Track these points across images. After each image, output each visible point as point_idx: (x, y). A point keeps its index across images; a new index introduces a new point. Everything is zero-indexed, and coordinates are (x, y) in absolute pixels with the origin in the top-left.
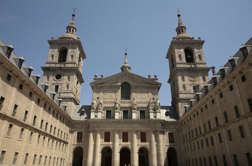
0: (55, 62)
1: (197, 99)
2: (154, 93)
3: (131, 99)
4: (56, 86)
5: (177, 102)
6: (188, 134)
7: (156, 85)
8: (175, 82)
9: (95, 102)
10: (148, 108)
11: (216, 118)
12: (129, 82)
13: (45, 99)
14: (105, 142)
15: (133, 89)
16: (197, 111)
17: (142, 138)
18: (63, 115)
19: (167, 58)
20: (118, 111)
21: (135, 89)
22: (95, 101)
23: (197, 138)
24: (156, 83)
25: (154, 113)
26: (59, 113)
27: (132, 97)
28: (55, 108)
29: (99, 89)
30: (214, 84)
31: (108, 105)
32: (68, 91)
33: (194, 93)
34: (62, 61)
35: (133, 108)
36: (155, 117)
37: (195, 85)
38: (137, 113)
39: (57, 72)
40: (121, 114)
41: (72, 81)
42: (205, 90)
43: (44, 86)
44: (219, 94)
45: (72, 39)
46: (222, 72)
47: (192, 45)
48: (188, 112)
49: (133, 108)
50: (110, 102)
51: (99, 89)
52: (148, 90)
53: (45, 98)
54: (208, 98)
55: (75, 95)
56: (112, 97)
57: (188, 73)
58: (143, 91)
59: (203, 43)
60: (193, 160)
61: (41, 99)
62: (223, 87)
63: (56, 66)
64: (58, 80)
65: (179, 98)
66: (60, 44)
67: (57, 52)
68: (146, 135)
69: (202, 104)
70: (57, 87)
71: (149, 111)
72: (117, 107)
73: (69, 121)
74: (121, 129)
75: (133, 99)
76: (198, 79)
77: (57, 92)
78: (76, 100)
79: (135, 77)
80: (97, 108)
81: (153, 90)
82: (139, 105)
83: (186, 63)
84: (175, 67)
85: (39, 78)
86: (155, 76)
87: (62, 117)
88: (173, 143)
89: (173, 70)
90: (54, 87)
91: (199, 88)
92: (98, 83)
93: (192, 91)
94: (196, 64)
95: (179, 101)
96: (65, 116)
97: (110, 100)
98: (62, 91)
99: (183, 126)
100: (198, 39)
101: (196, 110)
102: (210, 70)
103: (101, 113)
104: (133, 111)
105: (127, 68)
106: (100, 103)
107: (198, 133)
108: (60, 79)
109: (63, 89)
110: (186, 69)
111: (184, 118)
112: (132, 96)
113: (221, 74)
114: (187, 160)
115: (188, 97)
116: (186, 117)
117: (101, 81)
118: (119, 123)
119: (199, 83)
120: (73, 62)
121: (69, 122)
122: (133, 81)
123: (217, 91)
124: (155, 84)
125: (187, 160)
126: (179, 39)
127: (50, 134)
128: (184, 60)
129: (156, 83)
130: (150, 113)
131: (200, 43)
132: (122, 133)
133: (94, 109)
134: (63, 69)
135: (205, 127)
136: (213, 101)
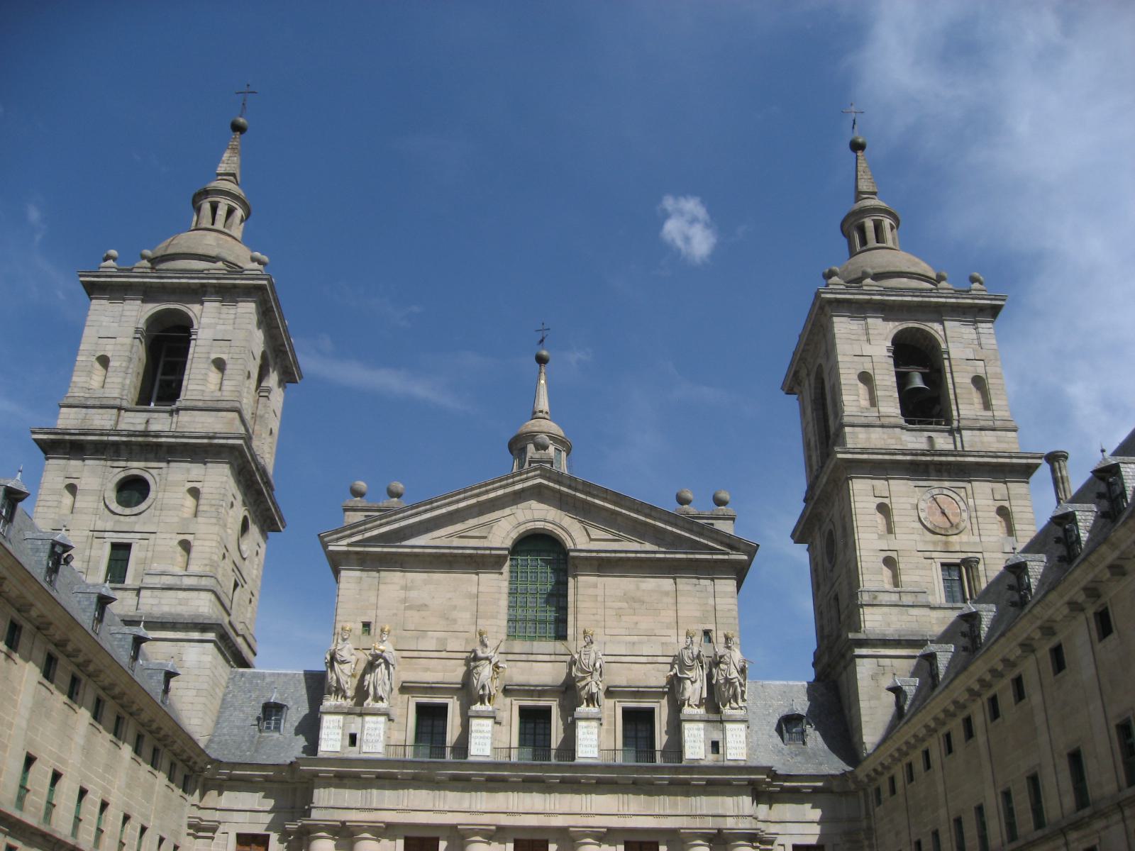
0: (112, 402)
1: (964, 641)
3: (570, 637)
4: (115, 547)
5: (848, 657)
8: (839, 533)
9: (346, 651)
10: (673, 689)
11: (1075, 759)
12: (559, 531)
13: (47, 629)
16: (965, 714)
18: (154, 726)
19: (790, 392)
20: (487, 707)
22: (349, 646)
24: (722, 543)
25: (707, 721)
26: (127, 716)
27: (579, 623)
28: (106, 683)
30: (1065, 553)
31: (427, 669)
32: (188, 582)
33: (950, 605)
34: (154, 397)
35: (583, 693)
36: (715, 746)
37: (955, 558)
38: (604, 722)
39: (122, 464)
40: (504, 729)
41: (214, 521)
42: (1011, 588)
43: (48, 547)
44: (1090, 612)
45: (220, 264)
46: (1109, 485)
48: (914, 720)
50: (444, 654)
53: (51, 624)
54: (1030, 638)
55: (227, 603)
56: (455, 621)
57: (910, 482)
61: (27, 627)
62: (1113, 574)
63: (122, 426)
64: (128, 511)
65: (861, 636)
66: (147, 293)
67: (128, 341)
69: (993, 671)
70: (121, 552)
71: (680, 711)
72: (483, 687)
73: (190, 763)
74: (505, 821)
75: (581, 636)
77: (119, 586)
78: (232, 634)
80: (361, 693)
82: (622, 676)
84: (837, 449)
85: (21, 500)
87: (148, 738)
89: (822, 467)
90: (103, 554)
91: (978, 576)
92: (367, 535)
95: (858, 651)
96: (166, 736)
97: (437, 639)
98: (150, 581)
99: (879, 802)
101: (964, 707)
102: (1037, 466)
103: (382, 719)
104: (583, 709)
105: (545, 448)
106: (376, 657)
108: (143, 506)
109: (156, 567)
111: (891, 756)
112: (576, 619)
113: (1100, 496)
115: (915, 626)
116: (899, 750)
118: (491, 785)
119: (975, 543)
120: (223, 405)
121: (186, 771)
123: (1081, 598)
126: (859, 280)
127: (70, 841)
133: (339, 691)
134: (159, 445)
135: (1010, 813)
136: (1057, 652)
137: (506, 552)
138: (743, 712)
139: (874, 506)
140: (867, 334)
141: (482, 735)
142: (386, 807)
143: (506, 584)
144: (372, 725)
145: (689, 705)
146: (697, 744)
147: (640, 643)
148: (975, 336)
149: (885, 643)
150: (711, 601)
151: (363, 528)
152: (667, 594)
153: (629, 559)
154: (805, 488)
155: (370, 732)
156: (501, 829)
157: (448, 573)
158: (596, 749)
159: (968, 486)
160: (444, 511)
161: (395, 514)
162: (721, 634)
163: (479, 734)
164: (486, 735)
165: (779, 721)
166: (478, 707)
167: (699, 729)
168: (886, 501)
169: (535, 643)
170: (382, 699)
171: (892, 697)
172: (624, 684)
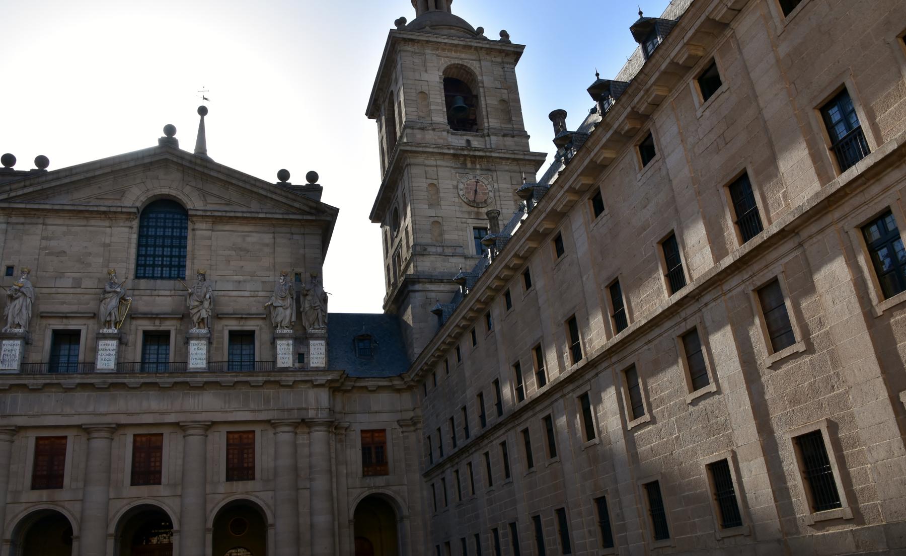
2: (302, 251)
6: (446, 428)
7: (313, 218)
12: (181, 197)
14: (34, 487)
15: (198, 232)
17: (236, 461)
21: (208, 233)
23: (482, 437)
29: (20, 227)
31: (63, 303)
36: (301, 357)
40: (129, 348)
47: (472, 57)
49: (195, 319)
50: (79, 290)
51: (17, 223)
52: (274, 238)
56: (89, 265)
57: (453, 171)
58: (249, 239)
59: (517, 52)
60: (463, 540)
68: (252, 445)
72: (110, 314)
74: (123, 420)
76: (497, 198)
79: (212, 173)
81: (295, 237)
83: (449, 127)
86: (312, 176)
88: (381, 477)
92: (13, 194)
93: (472, 249)
94: (487, 138)
100: (498, 38)
103: (19, 342)
107: (487, 413)
110: (446, 151)
112: (193, 263)
114: (438, 547)
117: (31, 185)
122: (204, 194)
124: (307, 209)
125: (438, 547)
128: (441, 118)
129: (311, 207)
130: (279, 342)
131: (508, 52)
132: (130, 439)
137: (135, 210)
138: (323, 331)
139: (425, 185)
140: (425, 66)
141: (108, 352)
142: (18, 413)
143: (135, 237)
144: (10, 348)
145: (282, 327)
146: (286, 356)
147: (245, 281)
148: (502, 73)
149: (432, 280)
150: (302, 251)
151: (8, 188)
152: (267, 245)
153: (237, 218)
154: (380, 183)
155: (7, 353)
156: (120, 426)
157: (85, 226)
158: (205, 362)
159: (494, 174)
160: (82, 177)
161: (38, 177)
162: (308, 275)
163: (104, 352)
164: (111, 352)
165: (354, 340)
166: (105, 331)
167: (288, 345)
168: (435, 182)
169: (159, 282)
170: (19, 326)
171: (436, 317)
172: (231, 312)
